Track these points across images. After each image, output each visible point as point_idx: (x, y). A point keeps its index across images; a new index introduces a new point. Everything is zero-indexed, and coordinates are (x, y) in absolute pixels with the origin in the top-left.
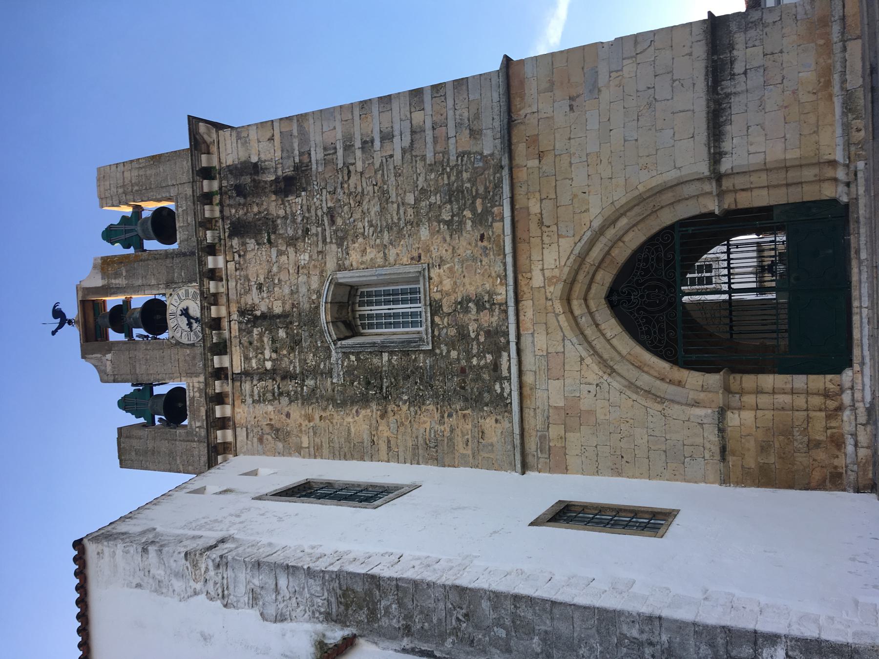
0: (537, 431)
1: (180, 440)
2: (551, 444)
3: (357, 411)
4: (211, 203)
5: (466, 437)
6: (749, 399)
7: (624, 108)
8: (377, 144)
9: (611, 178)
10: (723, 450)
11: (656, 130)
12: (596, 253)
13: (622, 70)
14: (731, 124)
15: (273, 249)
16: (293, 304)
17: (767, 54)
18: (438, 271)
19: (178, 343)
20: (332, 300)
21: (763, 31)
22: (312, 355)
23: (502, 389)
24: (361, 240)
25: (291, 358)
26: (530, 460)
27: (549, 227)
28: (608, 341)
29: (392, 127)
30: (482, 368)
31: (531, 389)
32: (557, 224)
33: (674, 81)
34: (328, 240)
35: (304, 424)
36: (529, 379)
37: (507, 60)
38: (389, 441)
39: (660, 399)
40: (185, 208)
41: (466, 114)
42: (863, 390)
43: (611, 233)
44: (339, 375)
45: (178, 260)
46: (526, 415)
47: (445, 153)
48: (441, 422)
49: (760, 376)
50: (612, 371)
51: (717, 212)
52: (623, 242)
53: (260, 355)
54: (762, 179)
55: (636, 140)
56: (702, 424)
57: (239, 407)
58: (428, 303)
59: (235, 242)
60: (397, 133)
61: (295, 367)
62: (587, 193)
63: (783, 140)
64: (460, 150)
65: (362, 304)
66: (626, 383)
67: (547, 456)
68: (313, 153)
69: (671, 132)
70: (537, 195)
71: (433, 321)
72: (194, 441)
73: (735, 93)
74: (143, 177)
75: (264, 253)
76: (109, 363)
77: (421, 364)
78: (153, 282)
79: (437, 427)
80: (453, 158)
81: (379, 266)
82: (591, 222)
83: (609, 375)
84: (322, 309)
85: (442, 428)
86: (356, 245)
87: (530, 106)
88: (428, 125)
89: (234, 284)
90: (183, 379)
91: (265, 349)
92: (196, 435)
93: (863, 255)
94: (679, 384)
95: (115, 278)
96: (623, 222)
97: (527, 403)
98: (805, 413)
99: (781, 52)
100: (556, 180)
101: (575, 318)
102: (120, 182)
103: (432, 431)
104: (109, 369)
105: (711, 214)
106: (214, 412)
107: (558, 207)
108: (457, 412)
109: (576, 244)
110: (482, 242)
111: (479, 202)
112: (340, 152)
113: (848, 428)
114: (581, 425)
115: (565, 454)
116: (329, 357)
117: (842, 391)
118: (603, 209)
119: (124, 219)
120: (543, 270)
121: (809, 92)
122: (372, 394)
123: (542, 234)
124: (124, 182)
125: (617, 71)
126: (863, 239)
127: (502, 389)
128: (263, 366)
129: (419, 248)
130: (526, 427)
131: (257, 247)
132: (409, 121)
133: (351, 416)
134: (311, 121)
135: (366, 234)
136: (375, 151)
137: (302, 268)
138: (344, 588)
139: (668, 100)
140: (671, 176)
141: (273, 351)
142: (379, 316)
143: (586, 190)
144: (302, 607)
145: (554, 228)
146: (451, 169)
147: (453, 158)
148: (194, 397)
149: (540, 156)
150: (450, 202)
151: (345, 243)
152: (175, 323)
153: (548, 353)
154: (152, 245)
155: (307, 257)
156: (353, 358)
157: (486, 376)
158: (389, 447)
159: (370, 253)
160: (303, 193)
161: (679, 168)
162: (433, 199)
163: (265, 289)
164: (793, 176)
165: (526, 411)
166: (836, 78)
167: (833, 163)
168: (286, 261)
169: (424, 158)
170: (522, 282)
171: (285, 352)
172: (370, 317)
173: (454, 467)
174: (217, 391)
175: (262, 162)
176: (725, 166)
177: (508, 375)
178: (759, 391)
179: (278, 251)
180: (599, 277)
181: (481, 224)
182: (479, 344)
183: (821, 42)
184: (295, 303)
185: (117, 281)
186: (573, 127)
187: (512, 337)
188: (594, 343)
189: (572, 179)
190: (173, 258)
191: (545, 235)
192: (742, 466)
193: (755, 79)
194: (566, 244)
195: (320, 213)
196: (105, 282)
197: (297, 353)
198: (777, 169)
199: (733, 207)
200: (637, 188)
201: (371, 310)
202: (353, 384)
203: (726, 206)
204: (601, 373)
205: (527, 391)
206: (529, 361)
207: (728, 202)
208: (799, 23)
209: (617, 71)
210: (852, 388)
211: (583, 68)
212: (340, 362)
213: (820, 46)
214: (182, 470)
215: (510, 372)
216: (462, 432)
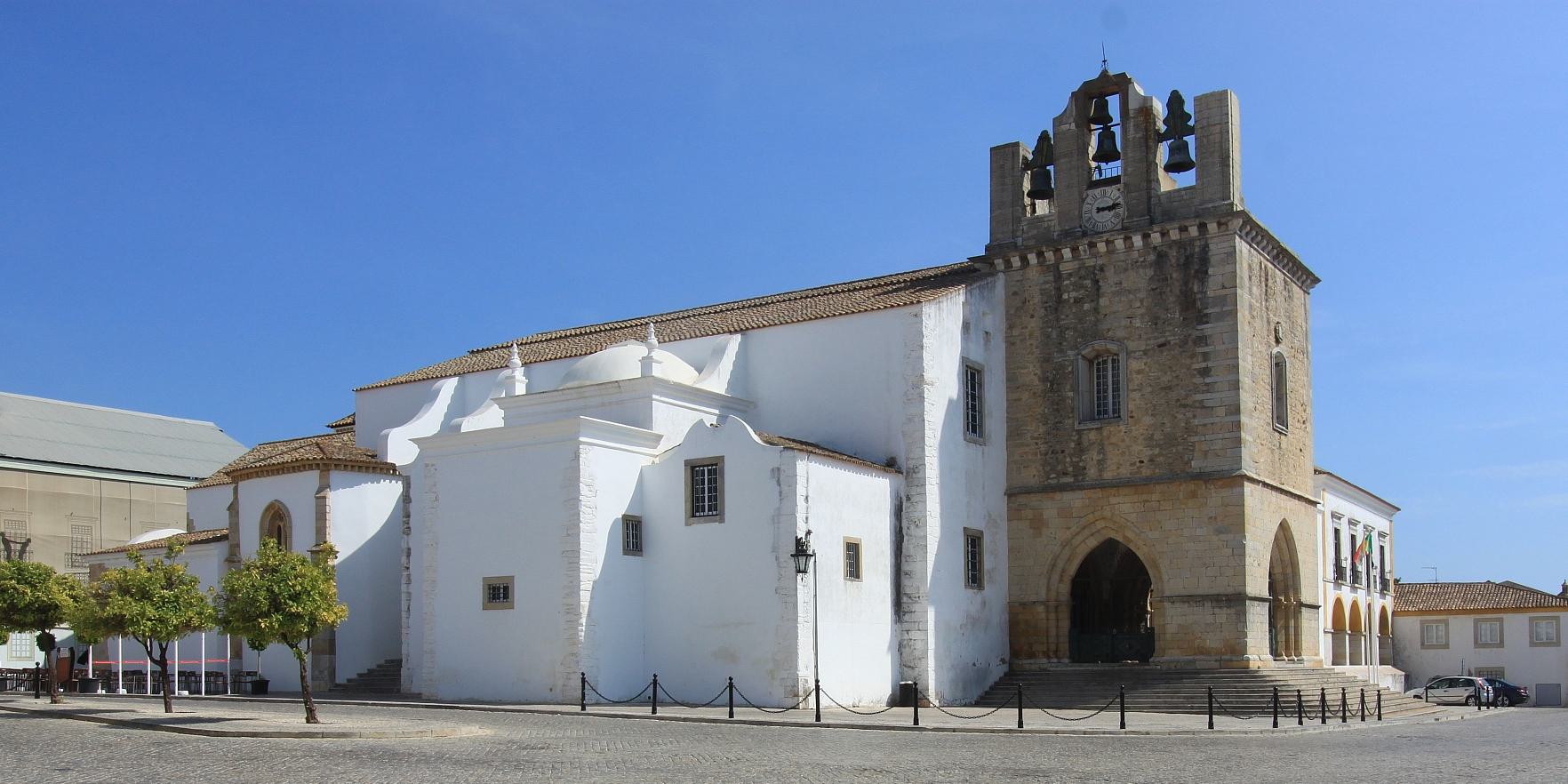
6: (1052, 616)
8: (1208, 380)
10: (1025, 604)
12: (1129, 534)
26: (1013, 498)
35: (1027, 330)
36: (1058, 496)
47: (1196, 434)
48: (1032, 438)
50: (1064, 546)
57: (1037, 272)
59: (1152, 257)
71: (1093, 429)
79: (1029, 435)
88: (1217, 420)
89: (1123, 258)
94: (1061, 581)
106: (1032, 252)
112: (1206, 349)
113: (1038, 661)
130: (1032, 495)
140: (1165, 577)
155: (1138, 325)
157: (1060, 467)
166: (1202, 657)
169: (1194, 416)
170: (1113, 491)
171: (1074, 311)
178: (1058, 620)
181: (1151, 460)
182: (1078, 462)
183: (1223, 650)
193: (1210, 619)
195: (1167, 334)
206: (1067, 497)
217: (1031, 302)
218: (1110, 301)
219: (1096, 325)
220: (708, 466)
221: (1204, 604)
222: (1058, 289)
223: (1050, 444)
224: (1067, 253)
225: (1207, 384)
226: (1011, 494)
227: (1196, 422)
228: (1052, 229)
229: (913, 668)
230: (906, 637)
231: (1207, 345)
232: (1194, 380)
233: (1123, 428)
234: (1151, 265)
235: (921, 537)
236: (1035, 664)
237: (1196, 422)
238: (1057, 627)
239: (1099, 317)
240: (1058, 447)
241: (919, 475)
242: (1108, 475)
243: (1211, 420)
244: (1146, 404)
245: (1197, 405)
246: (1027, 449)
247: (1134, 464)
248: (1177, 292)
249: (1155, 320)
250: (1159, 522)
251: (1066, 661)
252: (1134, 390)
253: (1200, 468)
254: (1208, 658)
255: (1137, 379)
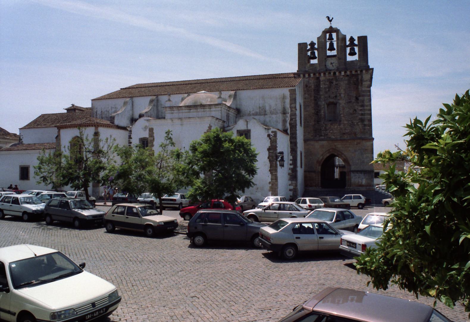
104: (321, 40)
149: (357, 144)
156: (323, 107)
176: (352, 173)
196: (340, 39)
220: (245, 132)
224: (322, 74)
251: (321, 188)
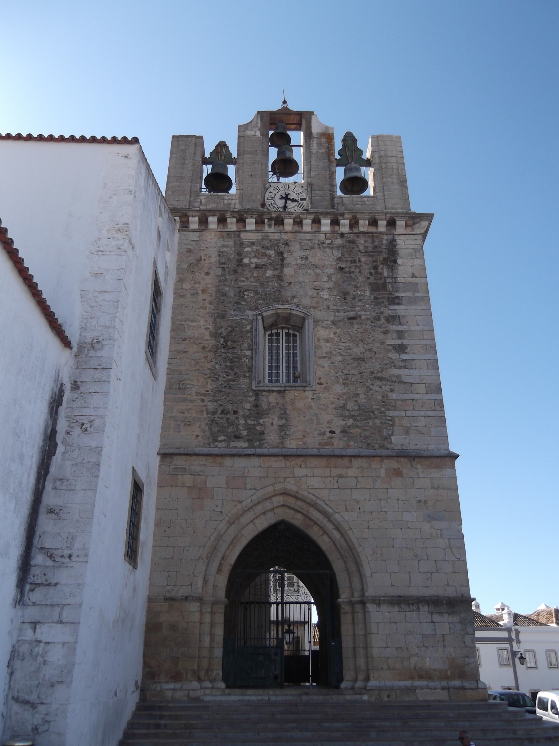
0: (189, 466)
1: (191, 186)
2: (179, 476)
3: (208, 328)
4: (369, 224)
5: (186, 412)
7: (416, 539)
8: (404, 357)
9: (368, 528)
10: (173, 599)
11: (399, 561)
12: (316, 515)
13: (442, 537)
14: (399, 611)
15: (332, 270)
16: (291, 283)
17: (443, 637)
18: (310, 398)
19: (266, 190)
20: (293, 314)
21: (460, 634)
22: (252, 295)
23: (221, 442)
24: (336, 339)
25: (250, 279)
26: (168, 459)
27: (337, 482)
28: (252, 521)
29: (416, 369)
30: (237, 427)
31: (220, 463)
32: (338, 488)
33: (431, 574)
34: (337, 314)
36: (228, 462)
37: (456, 456)
38: (185, 352)
39: (210, 556)
40: (367, 203)
41: (420, 424)
42: (212, 695)
43: (330, 527)
44: (236, 316)
45: (328, 195)
46: (201, 458)
47: (395, 408)
48: (198, 394)
49: (223, 626)
50: (231, 523)
51: (339, 600)
52: (322, 535)
53: (254, 255)
54: (360, 632)
55: (393, 547)
56: (191, 585)
57: (215, 236)
58: (287, 388)
60: (411, 372)
61: (243, 281)
62: (359, 511)
63: (385, 646)
64: (396, 419)
65: (288, 335)
66: (222, 533)
67: (170, 472)
68: (401, 307)
69: (397, 571)
70: (360, 475)
71: (273, 391)
72: (190, 197)
73: (419, 614)
74: (391, 173)
75: (330, 263)
76: (253, 133)
77: (241, 381)
78: (313, 173)
79: (194, 391)
80: (391, 413)
81: (315, 352)
82: (339, 513)
83: (228, 521)
84: (286, 306)
85: (194, 394)
86: (332, 336)
87: (423, 472)
89: (308, 238)
90: (238, 192)
91: (258, 259)
92: (194, 199)
93: (305, 698)
94: (219, 570)
95: (317, 144)
96: (336, 535)
97: (210, 459)
98: (197, 655)
99: (445, 646)
100: (369, 489)
101: (270, 498)
102: (389, 153)
103: (191, 386)
104: (250, 133)
105: (338, 596)
106: (213, 216)
107: (351, 489)
108: (205, 406)
109: (324, 501)
110: (329, 432)
111: (358, 430)
114: (193, 499)
115: (172, 486)
116: (251, 310)
117: (211, 681)
118: (347, 522)
119: (361, 152)
120: (307, 476)
121: (416, 664)
122: (220, 341)
123: (332, 477)
124: (389, 156)
125: (441, 534)
126: (315, 697)
127: (221, 442)
128: (246, 257)
129: (327, 383)
130: (193, 458)
131: (335, 258)
132: (419, 382)
133: (205, 324)
134: (424, 307)
135: (340, 344)
136: (400, 354)
137: (317, 293)
138: (104, 342)
139: (419, 569)
140: (367, 570)
141: (256, 265)
142: (278, 348)
143: (362, 510)
144: (90, 310)
145: (336, 486)
146: (384, 412)
147: (391, 413)
148: (224, 199)
150: (359, 410)
151: (334, 327)
152: (281, 189)
153: (246, 477)
154: (340, 173)
155: (325, 297)
157: (230, 429)
158: (180, 352)
159: (326, 346)
160: (372, 297)
161: (372, 576)
162: (362, 396)
163: (304, 262)
164: (361, 652)
165: (204, 458)
167: (367, 679)
168: (323, 280)
169: (392, 390)
170: (299, 461)
171: (255, 274)
172: (278, 341)
173: (165, 401)
174: (228, 219)
175: (397, 267)
177: (231, 446)
178: (212, 625)
179: (331, 274)
180: (299, 516)
181: (344, 432)
182: (255, 425)
183: (449, 673)
184: (292, 285)
185: (315, 145)
186: (405, 502)
187: (259, 451)
188: (251, 511)
189: (370, 500)
190: (330, 191)
191: (332, 479)
192: (161, 612)
193: (428, 629)
194: (324, 494)
195: (357, 309)
196: (315, 135)
197: (254, 284)
198: (366, 643)
199: (342, 611)
200: (361, 546)
201: (283, 342)
202: (229, 326)
203: (343, 606)
204: (230, 515)
205: (219, 460)
207: (346, 608)
208: (462, 659)
209: (441, 534)
210: (213, 688)
211: (445, 511)
212: (246, 317)
213: (447, 672)
214: (170, 186)
215: (232, 448)
216: (190, 409)
217: (207, 261)
218: (295, 272)
219: (280, 292)
221: (418, 608)
222: (239, 254)
223: (219, 402)
224: (251, 223)
225: (404, 361)
226: (164, 456)
227: (394, 396)
228: (232, 206)
229: (33, 706)
230: (29, 634)
231: (400, 324)
232: (390, 355)
233: (309, 394)
234: (338, 247)
235: (91, 449)
236: (181, 689)
237: (394, 396)
238: (212, 635)
239: (283, 284)
240: (230, 407)
241: (104, 353)
242: (292, 444)
243: (411, 396)
244: (337, 373)
245: (394, 379)
246: (191, 405)
247: (324, 434)
248: (366, 272)
249: (344, 295)
250: (358, 502)
252: (325, 357)
253: (402, 445)
254: (431, 684)
255: (326, 347)
